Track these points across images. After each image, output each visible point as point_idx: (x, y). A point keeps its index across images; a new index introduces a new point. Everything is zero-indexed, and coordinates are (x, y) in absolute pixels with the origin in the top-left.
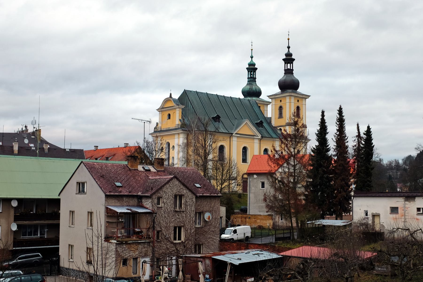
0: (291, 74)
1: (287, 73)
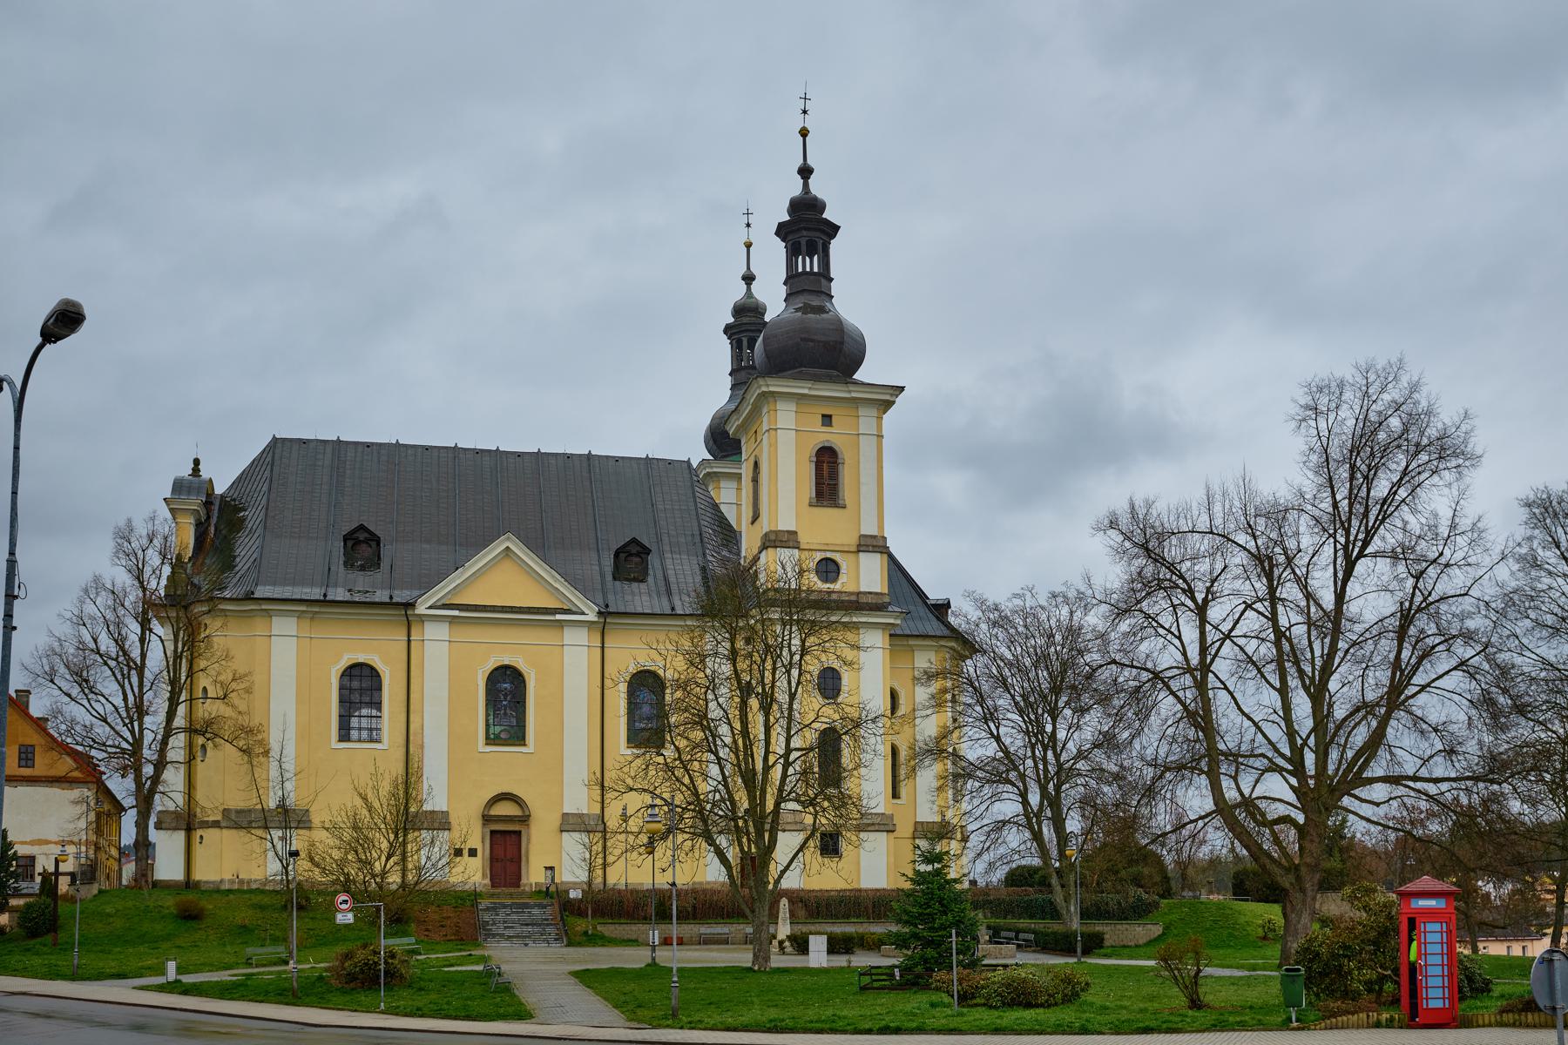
1: (798, 292)
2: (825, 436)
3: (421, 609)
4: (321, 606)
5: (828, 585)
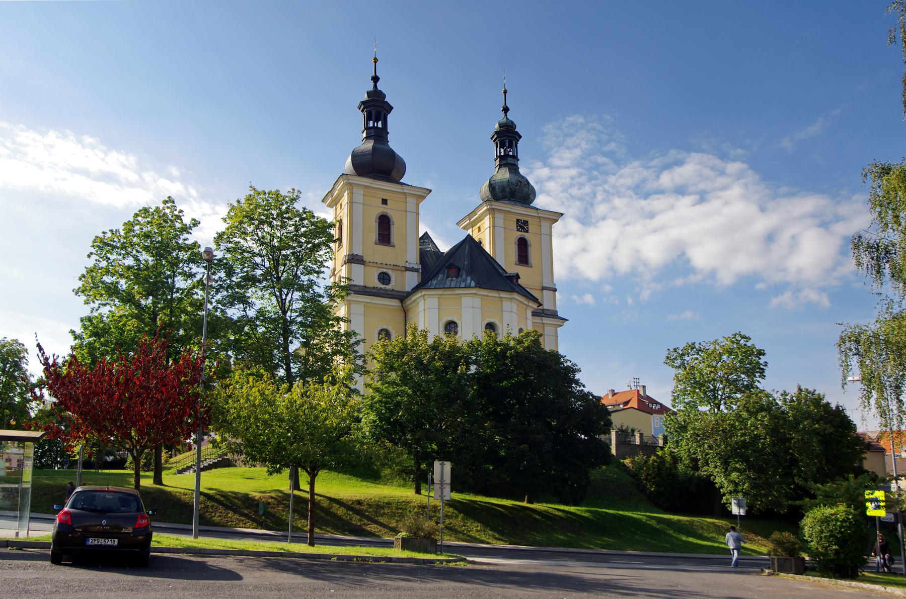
2: (381, 209)
5: (385, 286)
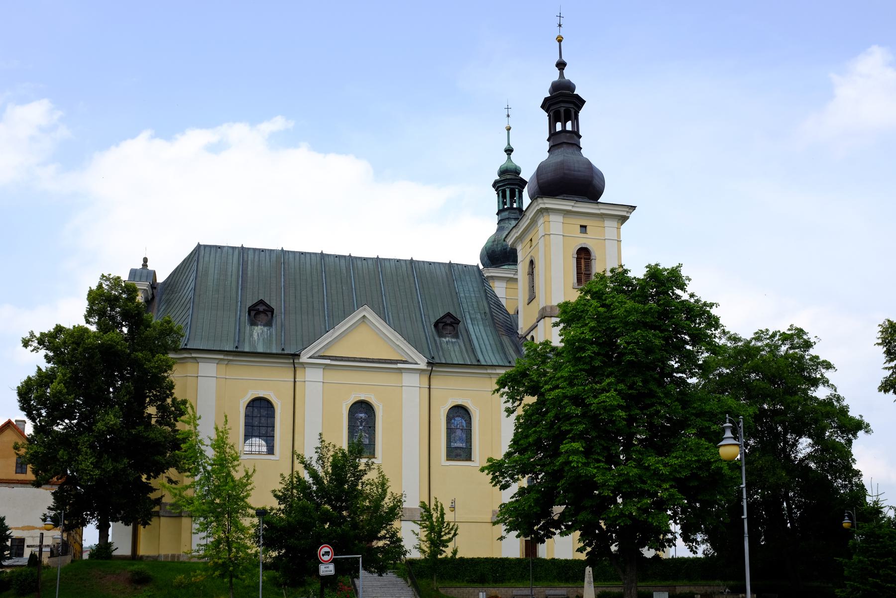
0: (565, 146)
3: (304, 358)
4: (234, 356)
